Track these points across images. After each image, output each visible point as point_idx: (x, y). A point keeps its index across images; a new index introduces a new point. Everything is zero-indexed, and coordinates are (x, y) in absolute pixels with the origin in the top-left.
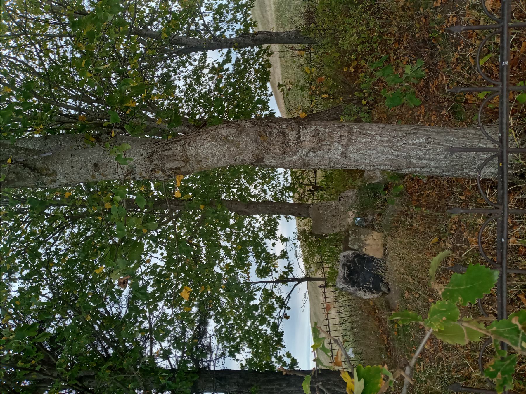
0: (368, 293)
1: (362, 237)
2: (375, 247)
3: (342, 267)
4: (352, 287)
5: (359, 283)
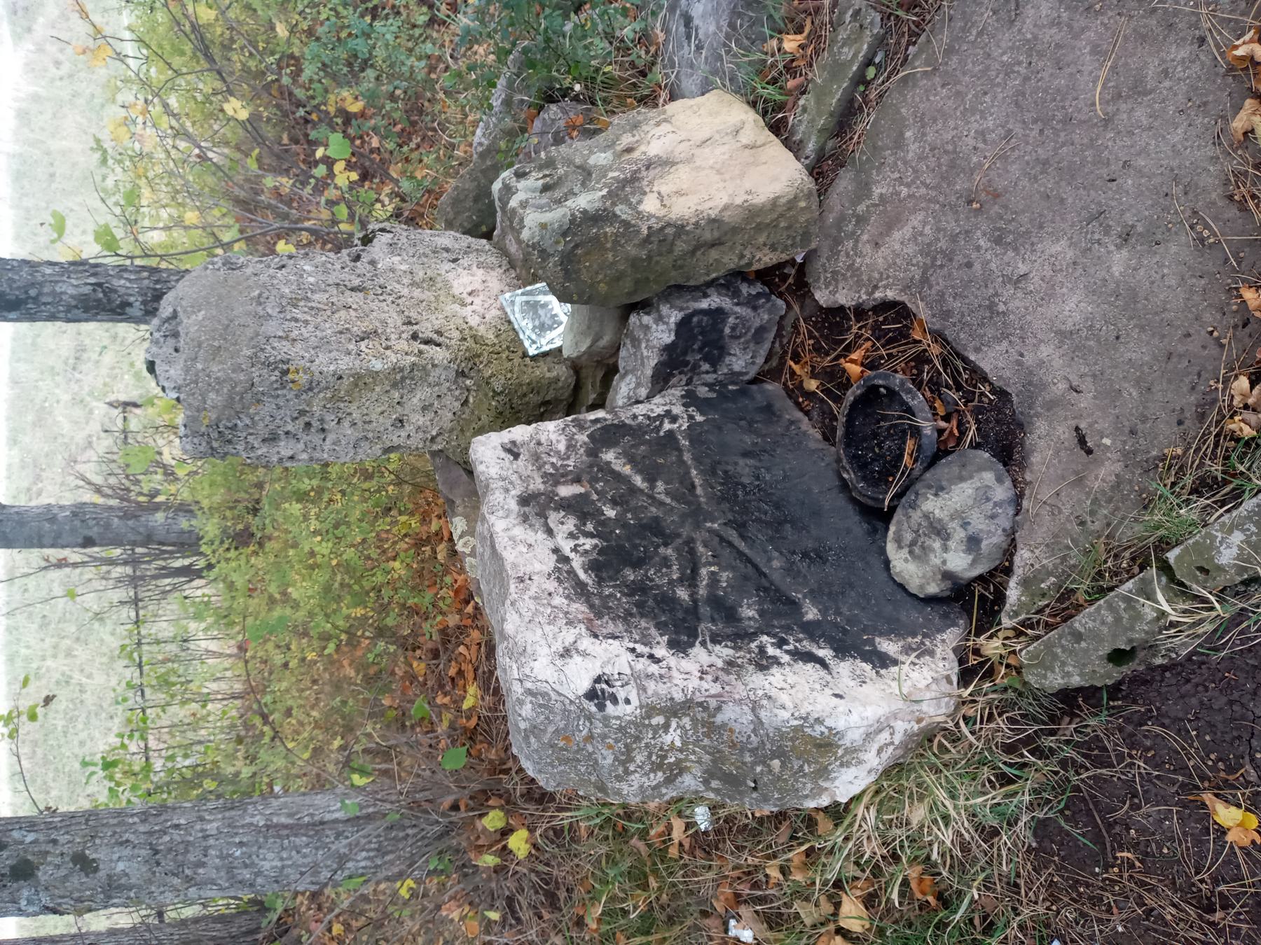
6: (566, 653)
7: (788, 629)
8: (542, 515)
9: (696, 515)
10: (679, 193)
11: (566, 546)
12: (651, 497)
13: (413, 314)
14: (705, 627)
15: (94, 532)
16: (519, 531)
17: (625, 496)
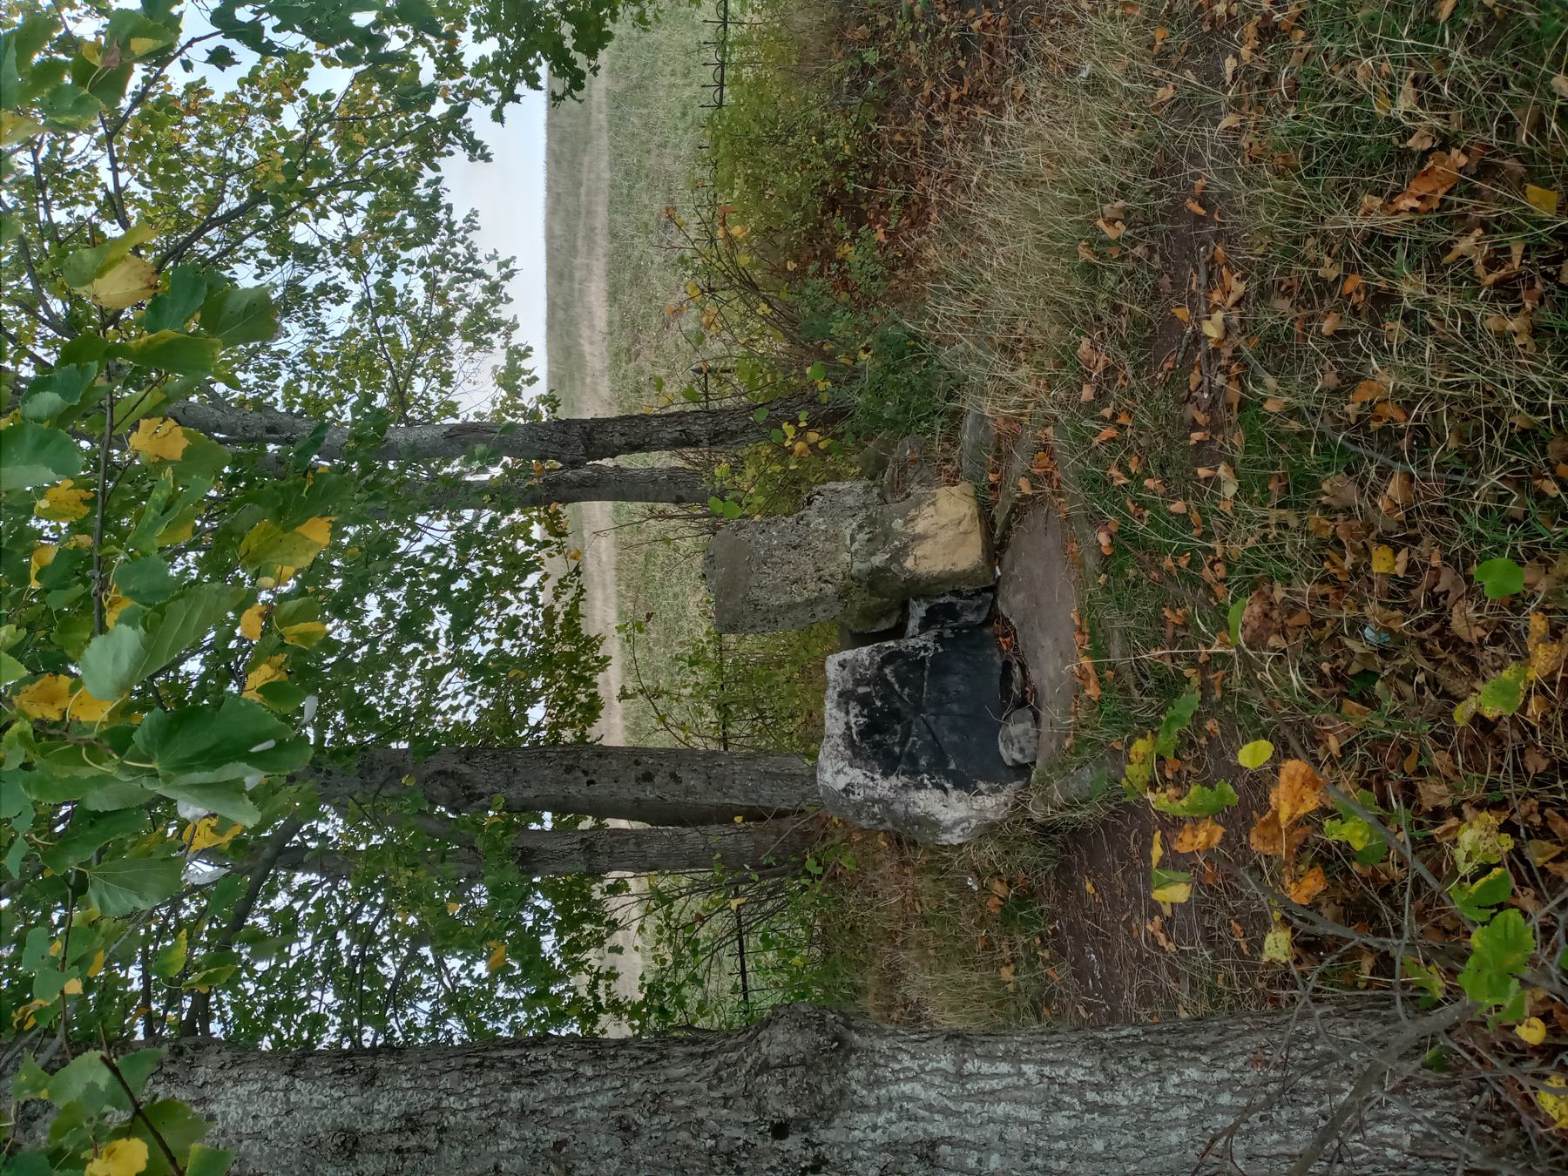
0: (954, 794)
1: (898, 524)
2: (946, 536)
3: (838, 705)
4: (885, 775)
5: (913, 759)
6: (838, 772)
7: (937, 772)
8: (847, 703)
9: (918, 708)
10: (925, 557)
11: (853, 720)
12: (900, 697)
13: (821, 565)
14: (901, 767)
15: (684, 492)
16: (834, 711)
17: (888, 693)
